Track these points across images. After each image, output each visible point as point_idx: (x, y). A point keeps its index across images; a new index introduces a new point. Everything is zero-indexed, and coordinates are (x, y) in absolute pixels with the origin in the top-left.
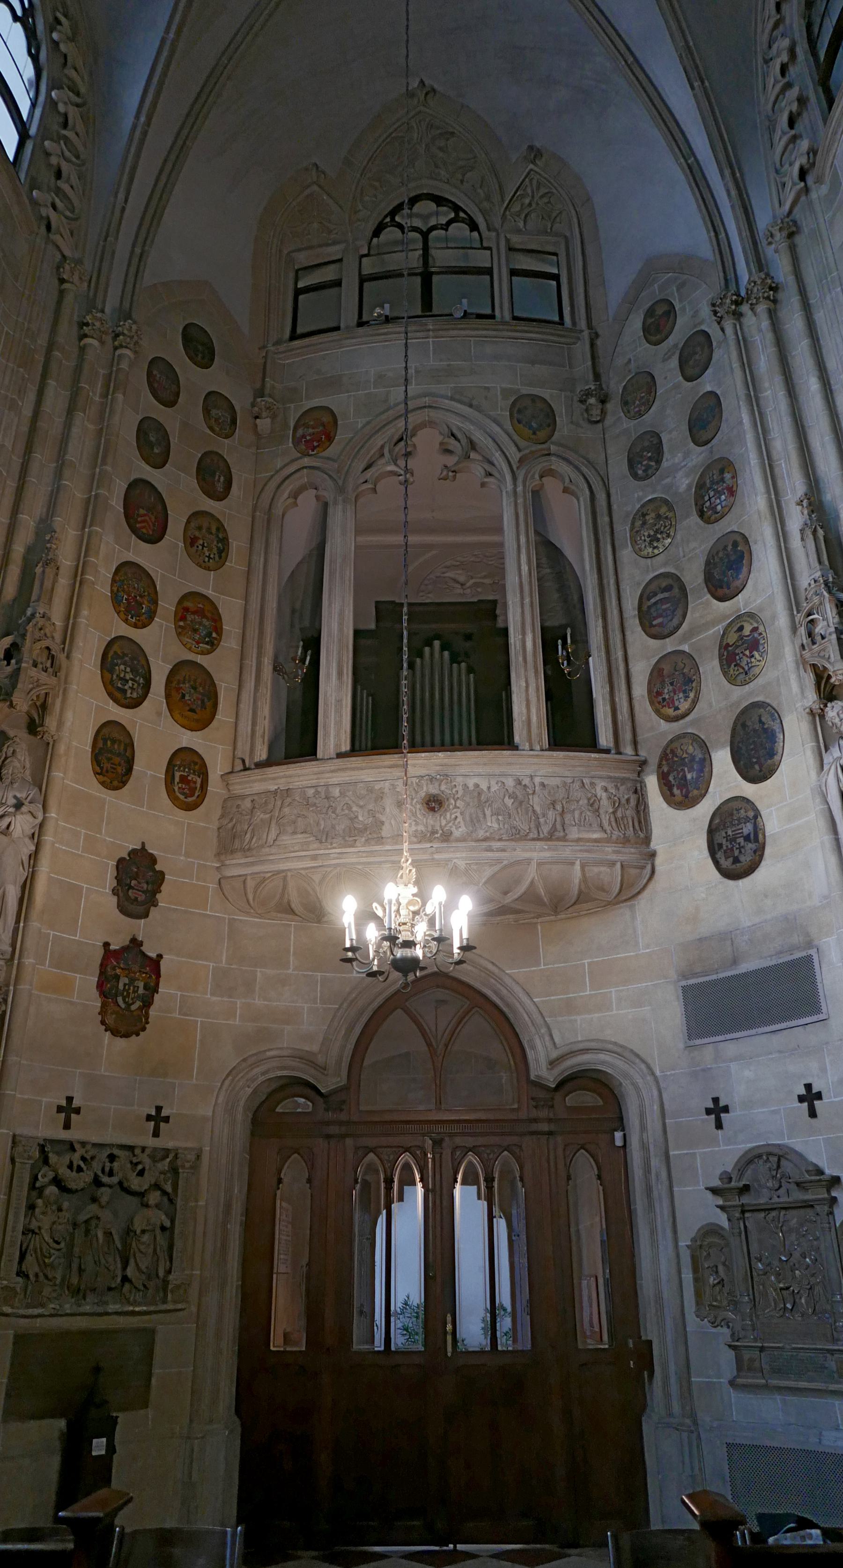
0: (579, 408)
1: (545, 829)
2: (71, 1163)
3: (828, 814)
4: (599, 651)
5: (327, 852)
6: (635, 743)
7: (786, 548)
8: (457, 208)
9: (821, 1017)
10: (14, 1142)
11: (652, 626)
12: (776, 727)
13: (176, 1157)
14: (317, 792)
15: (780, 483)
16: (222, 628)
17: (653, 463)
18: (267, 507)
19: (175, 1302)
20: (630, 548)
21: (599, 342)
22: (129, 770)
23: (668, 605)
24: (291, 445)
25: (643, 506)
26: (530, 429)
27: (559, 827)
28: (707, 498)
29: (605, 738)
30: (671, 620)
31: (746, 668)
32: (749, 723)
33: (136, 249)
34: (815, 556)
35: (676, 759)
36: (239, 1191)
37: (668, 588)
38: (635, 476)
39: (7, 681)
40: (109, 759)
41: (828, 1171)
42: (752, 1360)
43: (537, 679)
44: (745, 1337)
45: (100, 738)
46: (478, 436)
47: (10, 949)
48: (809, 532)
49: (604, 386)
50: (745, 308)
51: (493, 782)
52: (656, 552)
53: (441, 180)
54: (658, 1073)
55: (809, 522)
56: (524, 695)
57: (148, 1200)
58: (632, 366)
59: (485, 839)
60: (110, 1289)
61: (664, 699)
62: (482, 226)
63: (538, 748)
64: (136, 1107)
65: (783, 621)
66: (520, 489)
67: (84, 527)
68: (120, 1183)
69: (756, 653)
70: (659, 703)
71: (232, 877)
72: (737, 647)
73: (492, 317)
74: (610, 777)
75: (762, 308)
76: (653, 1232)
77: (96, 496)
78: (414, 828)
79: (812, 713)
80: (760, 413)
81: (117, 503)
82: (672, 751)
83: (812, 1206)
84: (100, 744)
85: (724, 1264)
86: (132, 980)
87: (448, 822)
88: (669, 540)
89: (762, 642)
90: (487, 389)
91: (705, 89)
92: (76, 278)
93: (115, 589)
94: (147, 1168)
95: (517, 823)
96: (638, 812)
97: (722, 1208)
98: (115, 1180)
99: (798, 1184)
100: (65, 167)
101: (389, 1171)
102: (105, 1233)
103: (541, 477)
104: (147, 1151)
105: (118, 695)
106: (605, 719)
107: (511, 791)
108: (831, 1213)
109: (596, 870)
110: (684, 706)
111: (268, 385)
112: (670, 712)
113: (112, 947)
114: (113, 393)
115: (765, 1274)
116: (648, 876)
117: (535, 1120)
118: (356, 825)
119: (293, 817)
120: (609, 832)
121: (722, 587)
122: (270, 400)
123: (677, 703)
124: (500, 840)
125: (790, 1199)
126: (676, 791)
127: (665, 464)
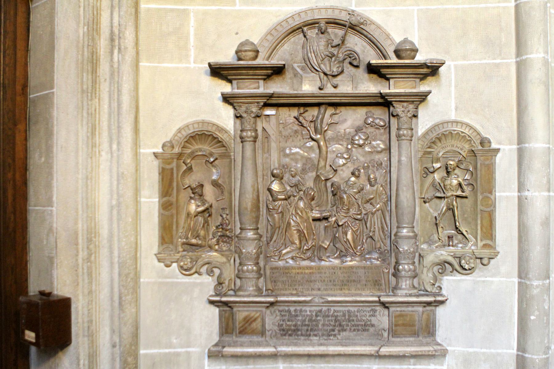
42: (248, 320)
44: (240, 289)
85: (215, 184)
97: (227, 99)
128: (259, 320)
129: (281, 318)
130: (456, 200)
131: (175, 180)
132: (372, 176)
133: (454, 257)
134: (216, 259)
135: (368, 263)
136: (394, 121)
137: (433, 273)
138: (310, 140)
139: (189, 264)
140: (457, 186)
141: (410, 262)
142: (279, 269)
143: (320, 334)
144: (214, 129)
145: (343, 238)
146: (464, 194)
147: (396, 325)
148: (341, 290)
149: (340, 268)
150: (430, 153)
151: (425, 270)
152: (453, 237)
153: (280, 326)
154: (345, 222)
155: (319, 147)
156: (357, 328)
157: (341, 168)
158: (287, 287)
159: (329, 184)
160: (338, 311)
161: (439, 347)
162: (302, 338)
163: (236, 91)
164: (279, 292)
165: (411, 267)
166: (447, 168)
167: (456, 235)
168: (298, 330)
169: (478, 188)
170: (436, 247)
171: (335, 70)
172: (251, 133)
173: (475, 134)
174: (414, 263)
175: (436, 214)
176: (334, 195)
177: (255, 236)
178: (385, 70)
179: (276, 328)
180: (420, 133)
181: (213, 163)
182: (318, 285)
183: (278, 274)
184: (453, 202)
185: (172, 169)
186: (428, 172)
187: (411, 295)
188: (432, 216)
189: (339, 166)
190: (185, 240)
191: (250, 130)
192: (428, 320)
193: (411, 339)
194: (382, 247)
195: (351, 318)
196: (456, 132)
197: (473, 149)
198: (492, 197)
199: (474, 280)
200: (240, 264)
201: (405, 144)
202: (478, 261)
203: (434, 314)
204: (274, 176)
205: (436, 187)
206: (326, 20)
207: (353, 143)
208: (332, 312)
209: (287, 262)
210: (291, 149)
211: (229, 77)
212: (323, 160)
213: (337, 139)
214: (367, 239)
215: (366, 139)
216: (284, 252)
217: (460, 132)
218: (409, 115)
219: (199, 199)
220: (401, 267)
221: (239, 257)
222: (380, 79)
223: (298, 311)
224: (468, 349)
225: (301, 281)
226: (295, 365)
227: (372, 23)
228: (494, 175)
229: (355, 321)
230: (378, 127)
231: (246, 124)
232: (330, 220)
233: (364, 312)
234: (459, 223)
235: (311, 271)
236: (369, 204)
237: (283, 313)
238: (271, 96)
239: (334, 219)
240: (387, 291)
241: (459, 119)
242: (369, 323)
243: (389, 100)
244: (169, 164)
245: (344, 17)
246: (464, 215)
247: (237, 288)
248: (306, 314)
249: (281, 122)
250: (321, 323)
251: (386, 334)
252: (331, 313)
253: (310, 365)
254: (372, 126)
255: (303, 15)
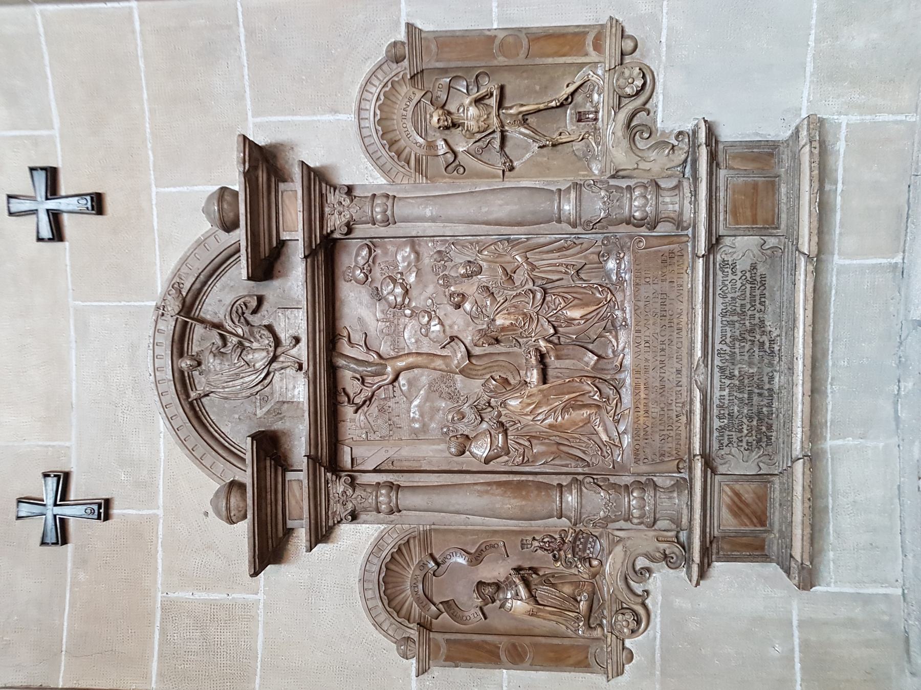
42: (739, 508)
44: (677, 521)
85: (476, 558)
128: (737, 487)
129: (735, 445)
130: (507, 108)
131: (468, 637)
132: (462, 271)
133: (619, 108)
134: (618, 565)
135: (627, 277)
136: (361, 230)
137: (649, 149)
138: (396, 384)
139: (627, 616)
140: (481, 106)
141: (628, 196)
142: (637, 447)
143: (770, 369)
144: (375, 561)
145: (579, 324)
146: (496, 93)
147: (755, 222)
148: (680, 329)
149: (638, 331)
150: (418, 161)
151: (643, 165)
152: (580, 112)
153: (749, 448)
154: (549, 322)
155: (409, 368)
156: (758, 298)
157: (447, 327)
158: (673, 434)
159: (477, 351)
160: (724, 336)
161: (804, 133)
162: (775, 404)
163: (305, 522)
164: (684, 448)
165: (637, 193)
166: (447, 128)
167: (575, 107)
168: (760, 412)
169: (483, 64)
170: (598, 144)
171: (268, 340)
172: (382, 494)
173: (380, 74)
174: (629, 187)
175: (535, 146)
176: (498, 341)
177: (574, 491)
178: (262, 249)
179: (755, 455)
180: (382, 181)
181: (440, 561)
182: (670, 374)
183: (647, 450)
184: (511, 115)
185: (448, 641)
186: (454, 165)
187: (695, 193)
188: (538, 154)
189: (444, 331)
190: (581, 624)
191: (377, 497)
192: (743, 157)
193: (783, 190)
194: (599, 249)
195: (738, 309)
196: (378, 112)
197: (409, 77)
198: (501, 35)
199: (665, 68)
200: (628, 519)
201: (400, 210)
202: (628, 59)
203: (733, 144)
204: (464, 453)
205: (482, 148)
206: (174, 358)
207: (402, 306)
208: (725, 347)
209: (625, 432)
210: (414, 420)
211: (281, 534)
212: (433, 361)
213: (395, 334)
214: (581, 279)
215: (394, 281)
216: (604, 438)
217: (378, 104)
218: (347, 202)
219: (504, 592)
220: (637, 214)
221: (614, 521)
222: (283, 258)
223: (722, 412)
224: (808, 74)
225: (662, 405)
226: (829, 417)
227: (177, 272)
228: (457, 34)
229: (743, 302)
230: (371, 260)
231: (366, 505)
232: (544, 350)
233: (726, 285)
234: (552, 101)
235: (642, 387)
236: (515, 276)
237: (726, 442)
238: (313, 459)
239: (542, 343)
240: (685, 239)
241: (354, 107)
242: (748, 274)
243: (318, 241)
244: (438, 647)
245: (168, 326)
246: (536, 92)
247: (674, 527)
248: (727, 398)
249: (364, 436)
250: (745, 368)
251: (772, 242)
252: (728, 349)
253: (829, 386)
254: (370, 271)
255: (165, 400)
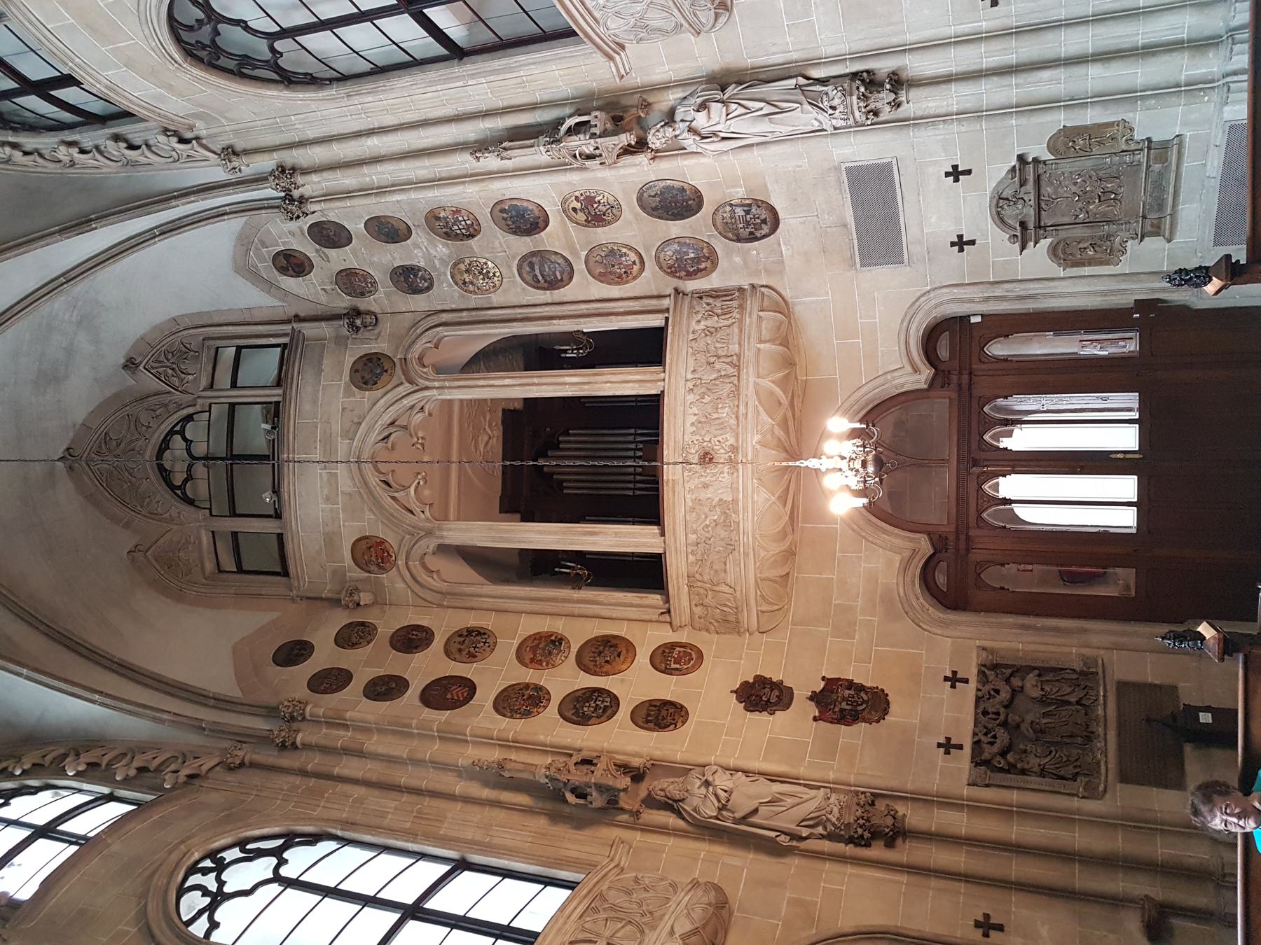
0: (363, 334)
1: (731, 370)
2: (988, 743)
3: (737, 150)
4: (581, 323)
5: (742, 545)
6: (659, 297)
7: (512, 172)
8: (172, 432)
9: (894, 162)
10: (974, 785)
11: (562, 280)
12: (662, 184)
13: (984, 666)
14: (692, 553)
15: (456, 173)
16: (547, 632)
17: (420, 273)
18: (439, 595)
19: (1096, 666)
20: (492, 295)
21: (302, 314)
22: (671, 703)
23: (546, 266)
24: (384, 576)
25: (457, 284)
26: (382, 374)
27: (729, 360)
28: (459, 232)
29: (656, 321)
30: (559, 264)
31: (608, 207)
32: (654, 205)
33: (211, 704)
34: (526, 150)
35: (676, 265)
36: (1010, 619)
37: (531, 265)
38: (428, 288)
39: (604, 796)
40: (664, 719)
41: (1013, 164)
42: (1152, 225)
43: (604, 374)
45: (646, 726)
46: (387, 418)
47: (822, 789)
48: (505, 154)
49: (346, 311)
50: (296, 193)
51: (691, 411)
52: (498, 274)
53: (146, 446)
54: (929, 288)
55: (496, 153)
56: (616, 385)
57: (1018, 686)
58: (328, 287)
59: (737, 418)
60: (1086, 714)
61: (625, 272)
62: (191, 410)
63: (663, 375)
64: (945, 697)
65: (574, 177)
66: (436, 384)
67: (467, 741)
68: (1006, 707)
69: (597, 199)
70: (628, 276)
71: (758, 622)
72: (589, 213)
73: (278, 403)
74: (688, 317)
75: (300, 180)
76: (1052, 296)
77: (438, 732)
78: (726, 475)
79: (653, 159)
80: (392, 186)
81: (442, 717)
82: (670, 268)
83: (1039, 176)
84: (651, 725)
85: (1079, 243)
86: (844, 699)
87: (723, 448)
88: (489, 263)
89: (588, 194)
90: (343, 409)
91: (97, 219)
92: (241, 753)
93: (518, 716)
94: (992, 687)
95: (726, 392)
96: (718, 297)
97: (1036, 243)
98: (1002, 710)
99: (1021, 186)
100: (136, 764)
101: (999, 502)
102: (1043, 717)
103: (424, 366)
104: (980, 687)
105: (609, 711)
106: (638, 320)
107: (698, 397)
108: (1044, 162)
109: (764, 331)
110: (633, 257)
111: (329, 595)
112: (636, 268)
113: (817, 714)
114: (346, 720)
115: (1088, 212)
116: (771, 291)
117: (960, 385)
118: (721, 521)
119: (712, 572)
120: (734, 320)
121: (538, 223)
122: (344, 593)
123: (630, 263)
124: (738, 406)
125: (1033, 192)
126: (703, 266)
127: (422, 264)
